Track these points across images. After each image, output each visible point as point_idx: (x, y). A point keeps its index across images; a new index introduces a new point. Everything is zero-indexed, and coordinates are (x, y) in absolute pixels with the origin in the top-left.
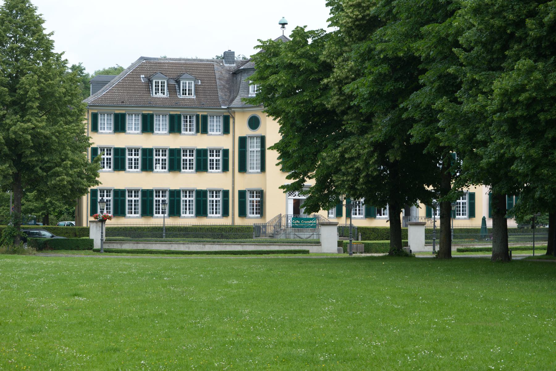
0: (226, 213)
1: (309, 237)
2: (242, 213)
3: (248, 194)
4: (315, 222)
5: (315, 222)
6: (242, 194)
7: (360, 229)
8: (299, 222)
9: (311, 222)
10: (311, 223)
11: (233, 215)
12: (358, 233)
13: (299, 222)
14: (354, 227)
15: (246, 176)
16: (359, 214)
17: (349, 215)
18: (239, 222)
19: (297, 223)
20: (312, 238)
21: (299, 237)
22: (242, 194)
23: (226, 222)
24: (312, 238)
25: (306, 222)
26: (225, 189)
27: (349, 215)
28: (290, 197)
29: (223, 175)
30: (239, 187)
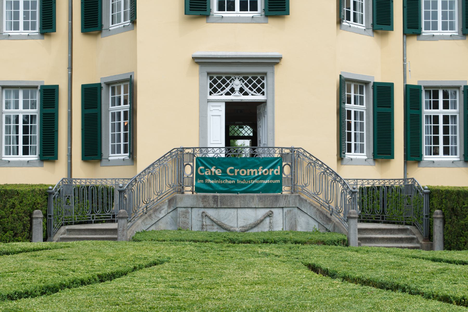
0: (49, 153)
1: (256, 225)
2: (92, 151)
3: (106, 97)
4: (276, 171)
5: (276, 171)
6: (91, 95)
7: (437, 196)
8: (218, 172)
9: (261, 171)
10: (263, 177)
11: (70, 156)
12: (431, 212)
13: (218, 172)
14: (418, 190)
15: (105, 42)
16: (446, 152)
17: (413, 155)
18: (83, 173)
19: (214, 177)
20: (265, 227)
21: (221, 226)
22: (91, 95)
23: (48, 176)
24: (265, 227)
25: (244, 172)
26: (48, 82)
27: (413, 155)
28: (215, 97)
29: (39, 45)
30: (85, 76)
